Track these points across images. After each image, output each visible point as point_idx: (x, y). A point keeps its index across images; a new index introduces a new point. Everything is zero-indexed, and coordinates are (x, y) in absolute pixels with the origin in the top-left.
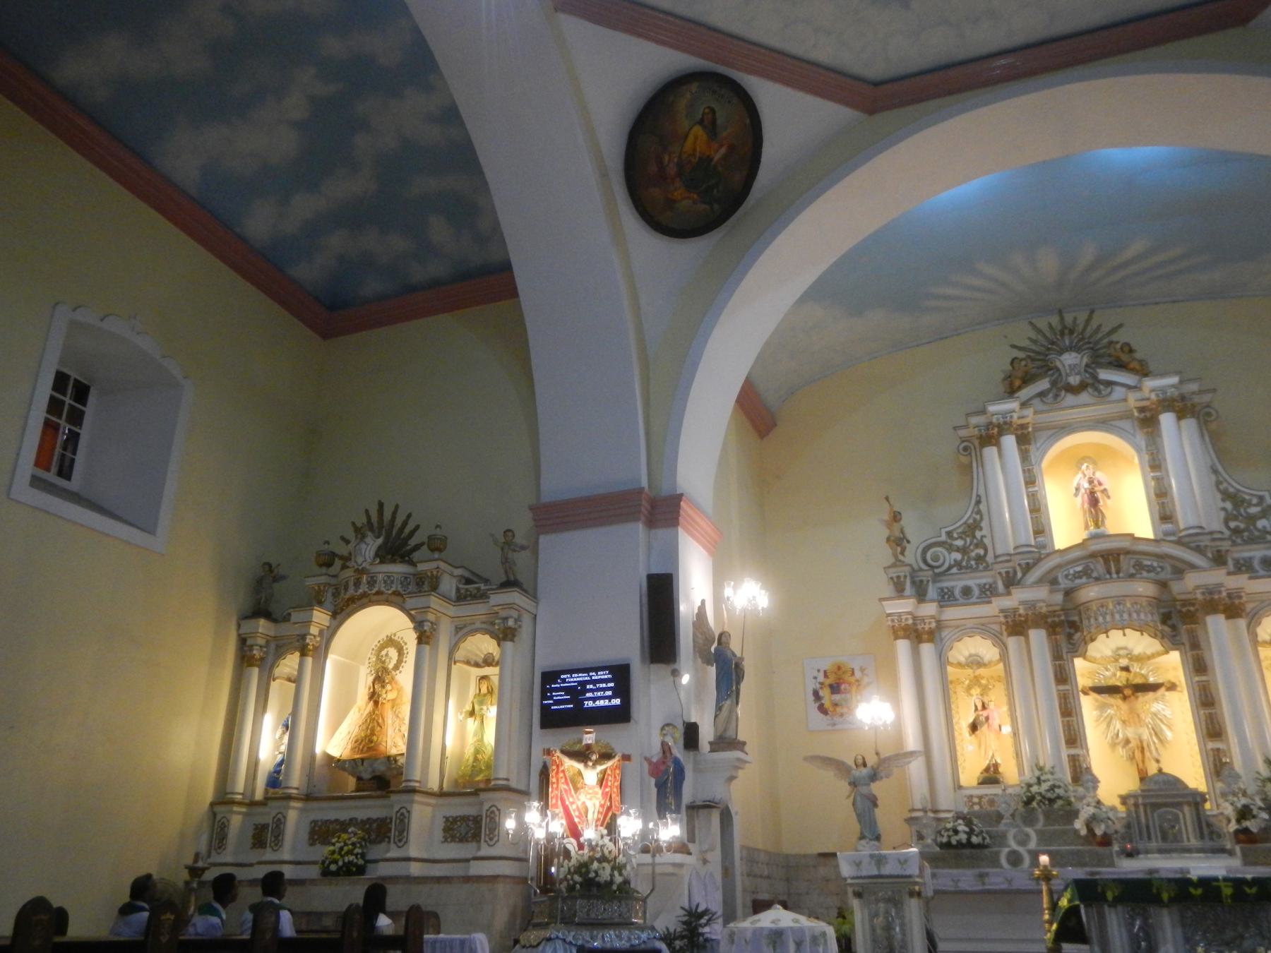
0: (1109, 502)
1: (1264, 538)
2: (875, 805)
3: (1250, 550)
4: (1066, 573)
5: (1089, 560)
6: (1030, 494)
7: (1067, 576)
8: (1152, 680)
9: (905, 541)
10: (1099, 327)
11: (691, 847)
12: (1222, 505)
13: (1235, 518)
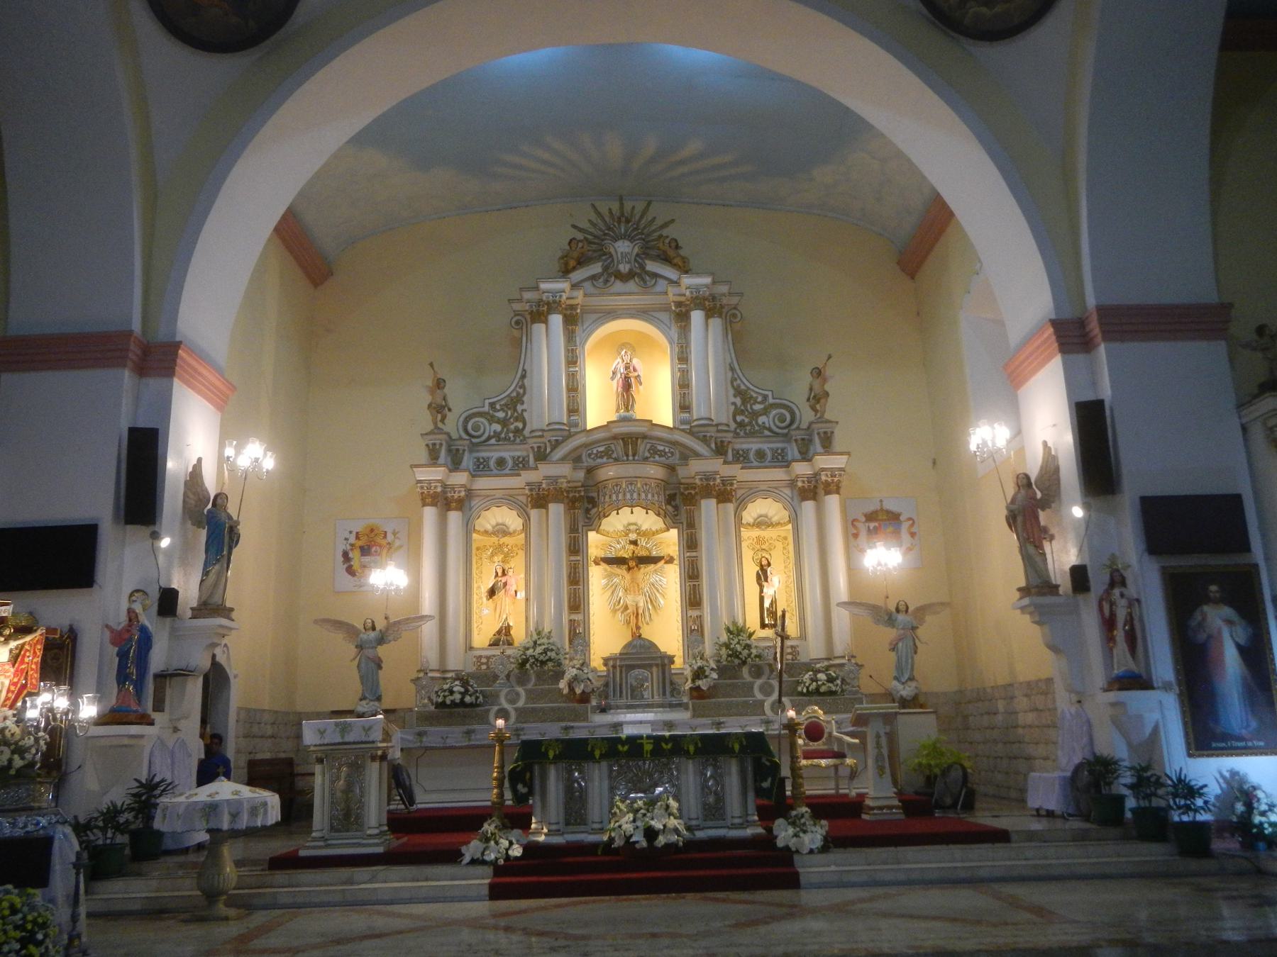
0: (641, 388)
1: (763, 433)
2: (380, 667)
3: (749, 443)
4: (590, 452)
7: (590, 455)
8: (654, 553)
9: (446, 409)
10: (655, 218)
11: (156, 716)
12: (732, 399)
13: (742, 413)
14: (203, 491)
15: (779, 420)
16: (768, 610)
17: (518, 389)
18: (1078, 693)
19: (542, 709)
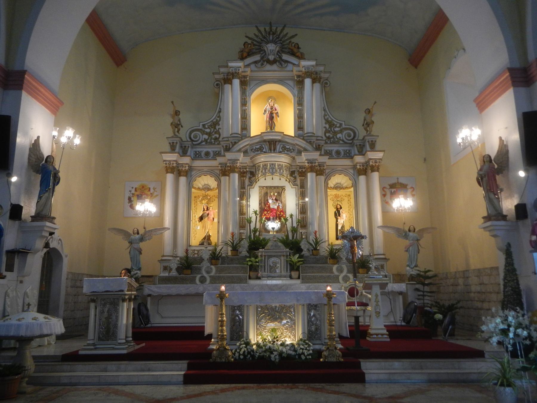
0: (278, 119)
2: (141, 253)
3: (331, 147)
4: (252, 148)
5: (263, 143)
6: (243, 110)
7: (252, 150)
9: (180, 126)
10: (287, 33)
12: (324, 125)
13: (329, 132)
14: (40, 154)
15: (347, 136)
17: (217, 118)
19: (223, 276)
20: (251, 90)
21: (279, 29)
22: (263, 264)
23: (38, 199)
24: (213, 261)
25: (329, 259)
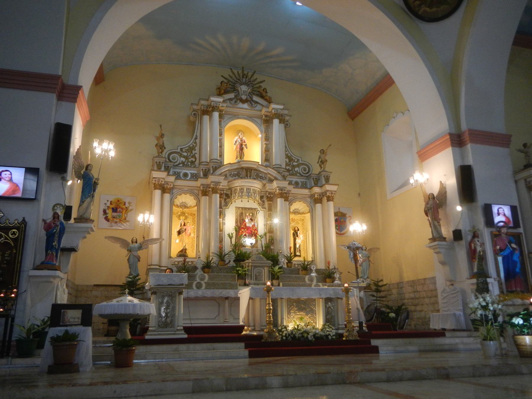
2: (139, 261)
3: (293, 178)
5: (241, 170)
7: (230, 175)
14: (81, 162)
16: (298, 249)
18: (451, 281)
20: (225, 123)
21: (250, 74)
22: (250, 273)
23: (80, 203)
24: (206, 270)
25: (302, 270)
